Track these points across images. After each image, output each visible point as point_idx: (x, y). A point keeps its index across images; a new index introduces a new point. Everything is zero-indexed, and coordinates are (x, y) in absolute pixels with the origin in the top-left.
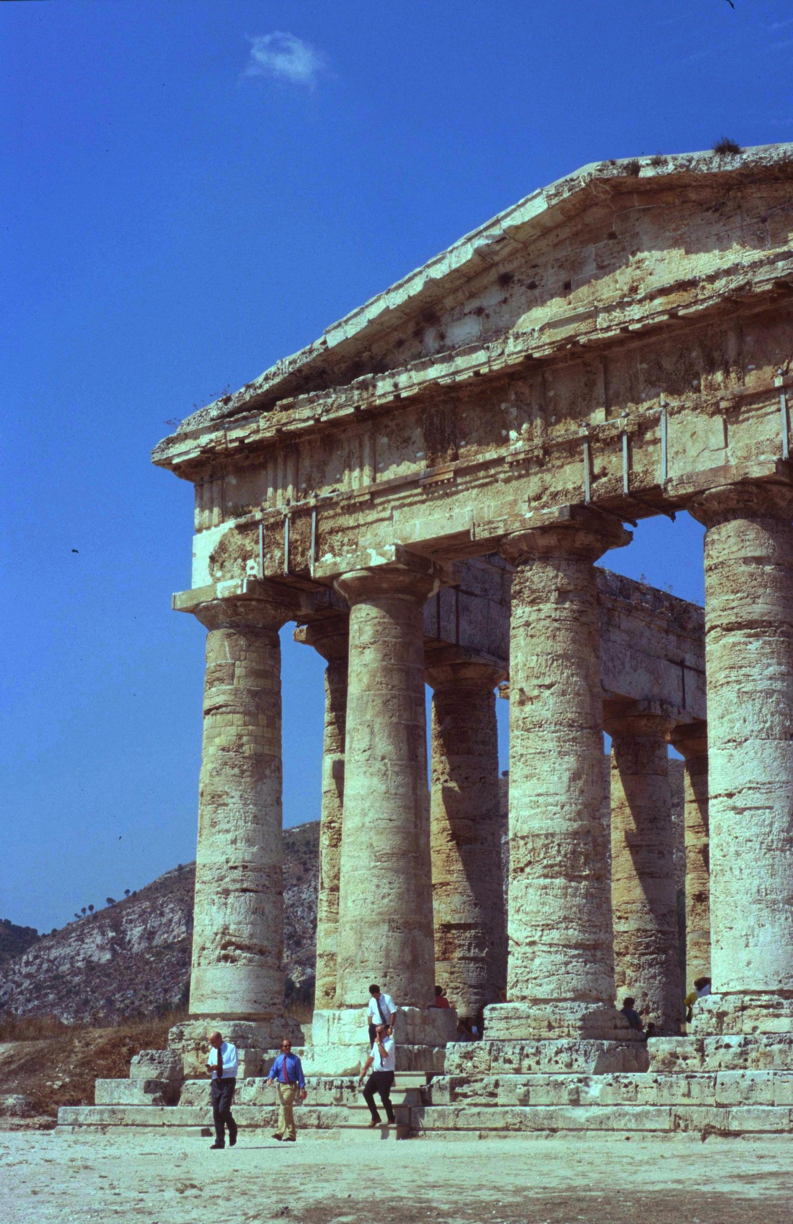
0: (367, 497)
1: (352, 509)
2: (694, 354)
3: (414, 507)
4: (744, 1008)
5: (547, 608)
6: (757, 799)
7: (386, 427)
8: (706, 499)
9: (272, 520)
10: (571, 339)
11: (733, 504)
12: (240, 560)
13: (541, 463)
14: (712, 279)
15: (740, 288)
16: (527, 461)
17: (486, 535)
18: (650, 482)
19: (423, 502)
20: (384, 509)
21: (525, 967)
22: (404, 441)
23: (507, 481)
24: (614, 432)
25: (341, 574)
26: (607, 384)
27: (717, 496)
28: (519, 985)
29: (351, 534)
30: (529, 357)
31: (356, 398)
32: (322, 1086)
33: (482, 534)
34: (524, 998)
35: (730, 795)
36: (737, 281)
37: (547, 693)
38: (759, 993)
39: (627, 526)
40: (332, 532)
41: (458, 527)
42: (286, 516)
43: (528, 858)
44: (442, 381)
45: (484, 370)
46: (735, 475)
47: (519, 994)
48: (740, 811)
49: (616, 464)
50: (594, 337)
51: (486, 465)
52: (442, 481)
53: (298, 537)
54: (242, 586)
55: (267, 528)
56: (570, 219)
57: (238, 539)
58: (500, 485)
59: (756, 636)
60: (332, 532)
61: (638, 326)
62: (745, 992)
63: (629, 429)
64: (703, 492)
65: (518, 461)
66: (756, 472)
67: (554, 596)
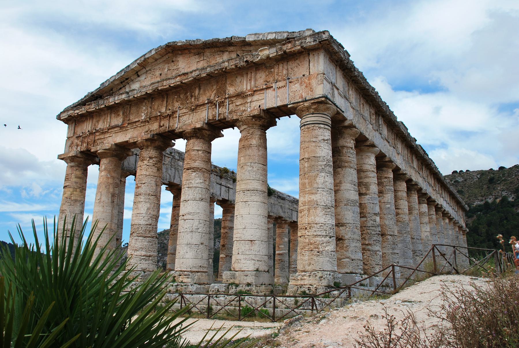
1: (103, 133)
4: (180, 275)
5: (146, 162)
6: (190, 217)
10: (157, 88)
11: (192, 135)
13: (148, 122)
14: (191, 72)
15: (198, 75)
16: (145, 121)
17: (132, 141)
18: (173, 128)
23: (140, 127)
24: (166, 114)
26: (167, 102)
27: (188, 132)
29: (102, 140)
30: (146, 93)
33: (132, 141)
35: (183, 216)
36: (197, 73)
37: (143, 185)
38: (185, 271)
39: (173, 141)
40: (98, 139)
41: (126, 139)
44: (126, 99)
45: (136, 96)
46: (193, 126)
48: (185, 220)
49: (165, 123)
50: (162, 88)
51: (136, 122)
55: (83, 138)
57: (76, 141)
58: (138, 128)
59: (195, 172)
60: (98, 139)
62: (181, 271)
63: (170, 113)
66: (198, 126)
67: (148, 159)
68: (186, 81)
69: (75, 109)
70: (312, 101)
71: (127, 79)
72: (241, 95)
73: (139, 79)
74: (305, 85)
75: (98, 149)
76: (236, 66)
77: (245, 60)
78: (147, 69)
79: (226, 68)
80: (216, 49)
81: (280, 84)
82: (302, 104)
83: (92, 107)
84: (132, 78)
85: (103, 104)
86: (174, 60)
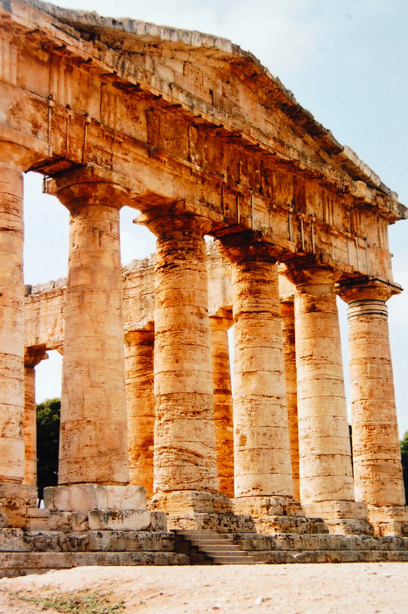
0: (121, 140)
2: (258, 171)
3: (141, 166)
7: (126, 101)
8: (272, 249)
9: (60, 113)
12: (31, 125)
19: (146, 164)
20: (126, 154)
21: (207, 471)
22: (135, 118)
25: (112, 183)
28: (204, 480)
31: (139, 77)
32: (154, 538)
34: (206, 488)
42: (70, 116)
43: (206, 407)
45: (204, 116)
47: (204, 486)
50: (247, 138)
52: (162, 160)
53: (75, 136)
54: (49, 150)
56: (218, 59)
61: (263, 148)
64: (273, 245)
65: (197, 175)
68: (282, 156)
69: (59, 24)
70: (393, 289)
71: (155, 46)
72: (327, 229)
73: (169, 63)
74: (378, 260)
75: (115, 178)
76: (336, 184)
77: (346, 184)
78: (191, 59)
79: (326, 178)
80: (291, 122)
81: (361, 242)
82: (386, 286)
83: (108, 61)
84: (165, 52)
85: (135, 76)
86: (231, 80)
